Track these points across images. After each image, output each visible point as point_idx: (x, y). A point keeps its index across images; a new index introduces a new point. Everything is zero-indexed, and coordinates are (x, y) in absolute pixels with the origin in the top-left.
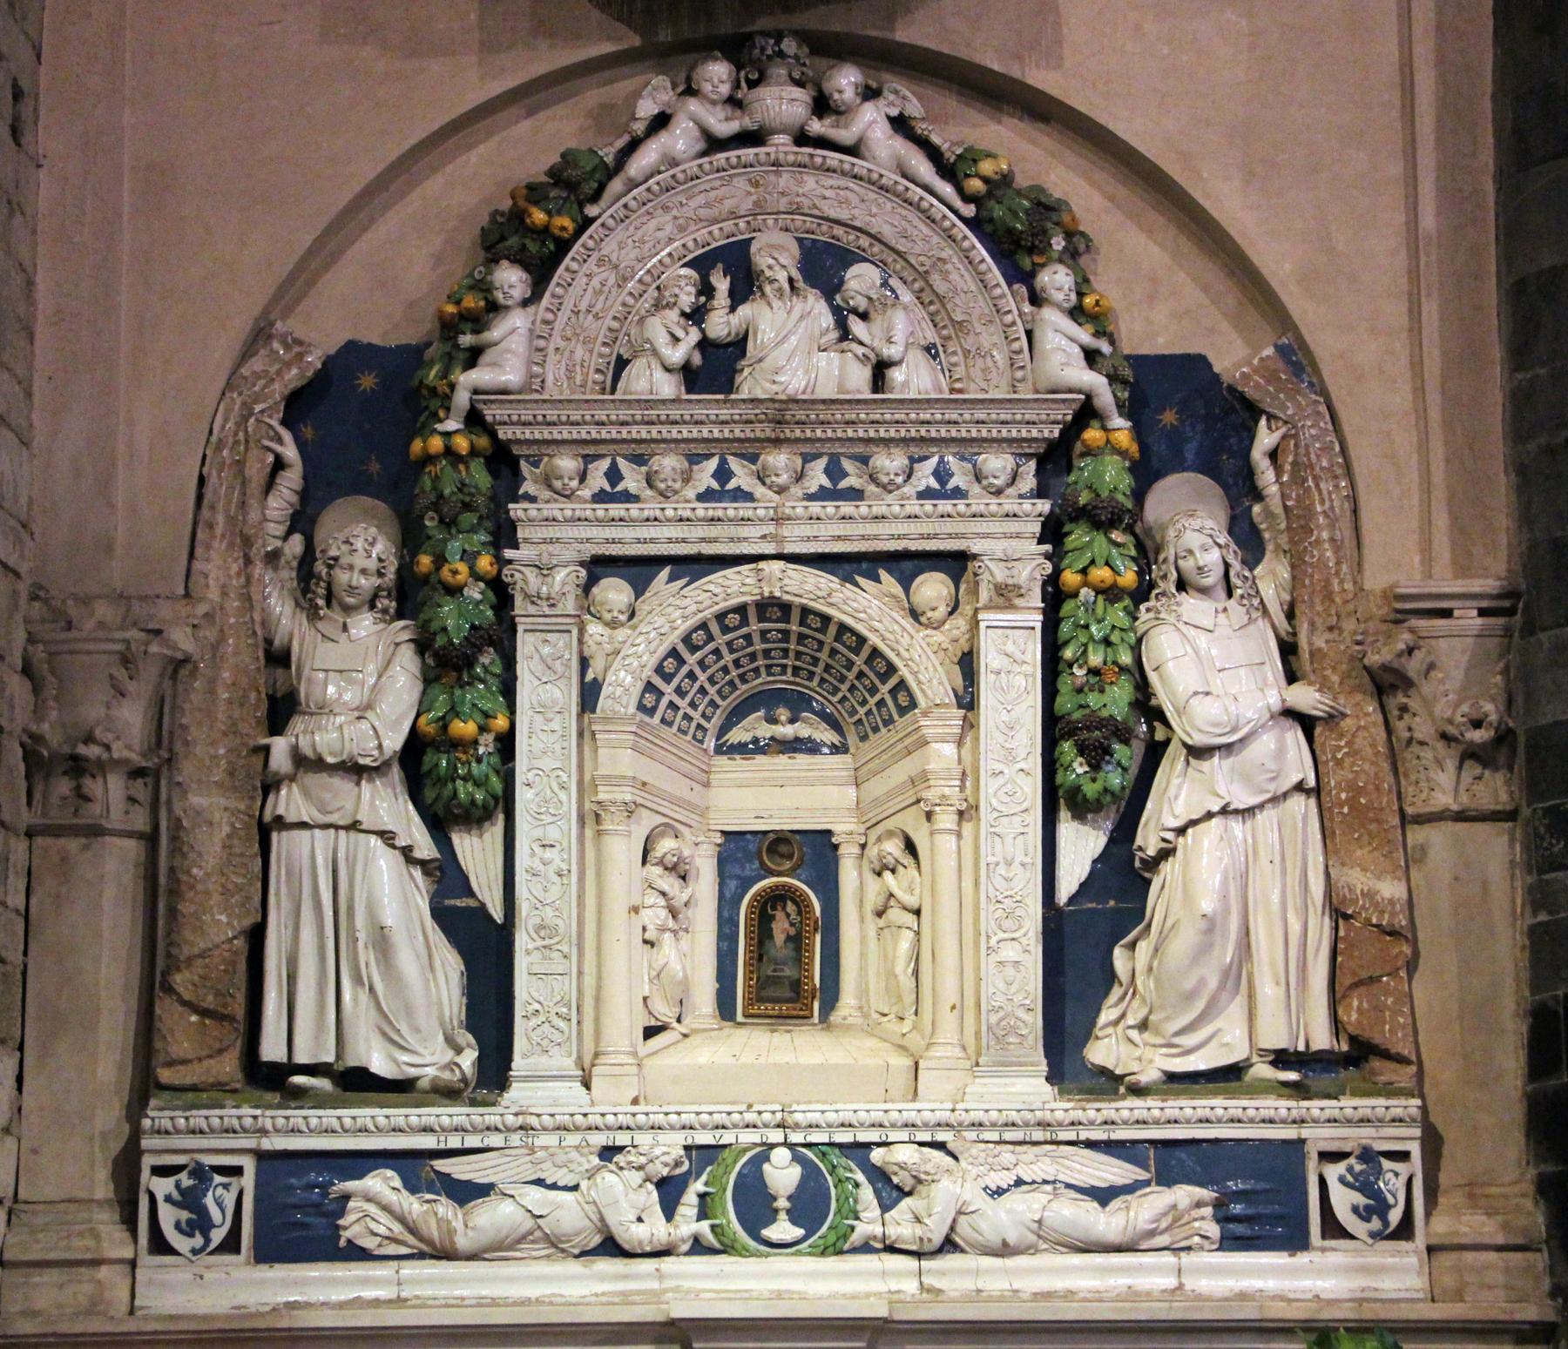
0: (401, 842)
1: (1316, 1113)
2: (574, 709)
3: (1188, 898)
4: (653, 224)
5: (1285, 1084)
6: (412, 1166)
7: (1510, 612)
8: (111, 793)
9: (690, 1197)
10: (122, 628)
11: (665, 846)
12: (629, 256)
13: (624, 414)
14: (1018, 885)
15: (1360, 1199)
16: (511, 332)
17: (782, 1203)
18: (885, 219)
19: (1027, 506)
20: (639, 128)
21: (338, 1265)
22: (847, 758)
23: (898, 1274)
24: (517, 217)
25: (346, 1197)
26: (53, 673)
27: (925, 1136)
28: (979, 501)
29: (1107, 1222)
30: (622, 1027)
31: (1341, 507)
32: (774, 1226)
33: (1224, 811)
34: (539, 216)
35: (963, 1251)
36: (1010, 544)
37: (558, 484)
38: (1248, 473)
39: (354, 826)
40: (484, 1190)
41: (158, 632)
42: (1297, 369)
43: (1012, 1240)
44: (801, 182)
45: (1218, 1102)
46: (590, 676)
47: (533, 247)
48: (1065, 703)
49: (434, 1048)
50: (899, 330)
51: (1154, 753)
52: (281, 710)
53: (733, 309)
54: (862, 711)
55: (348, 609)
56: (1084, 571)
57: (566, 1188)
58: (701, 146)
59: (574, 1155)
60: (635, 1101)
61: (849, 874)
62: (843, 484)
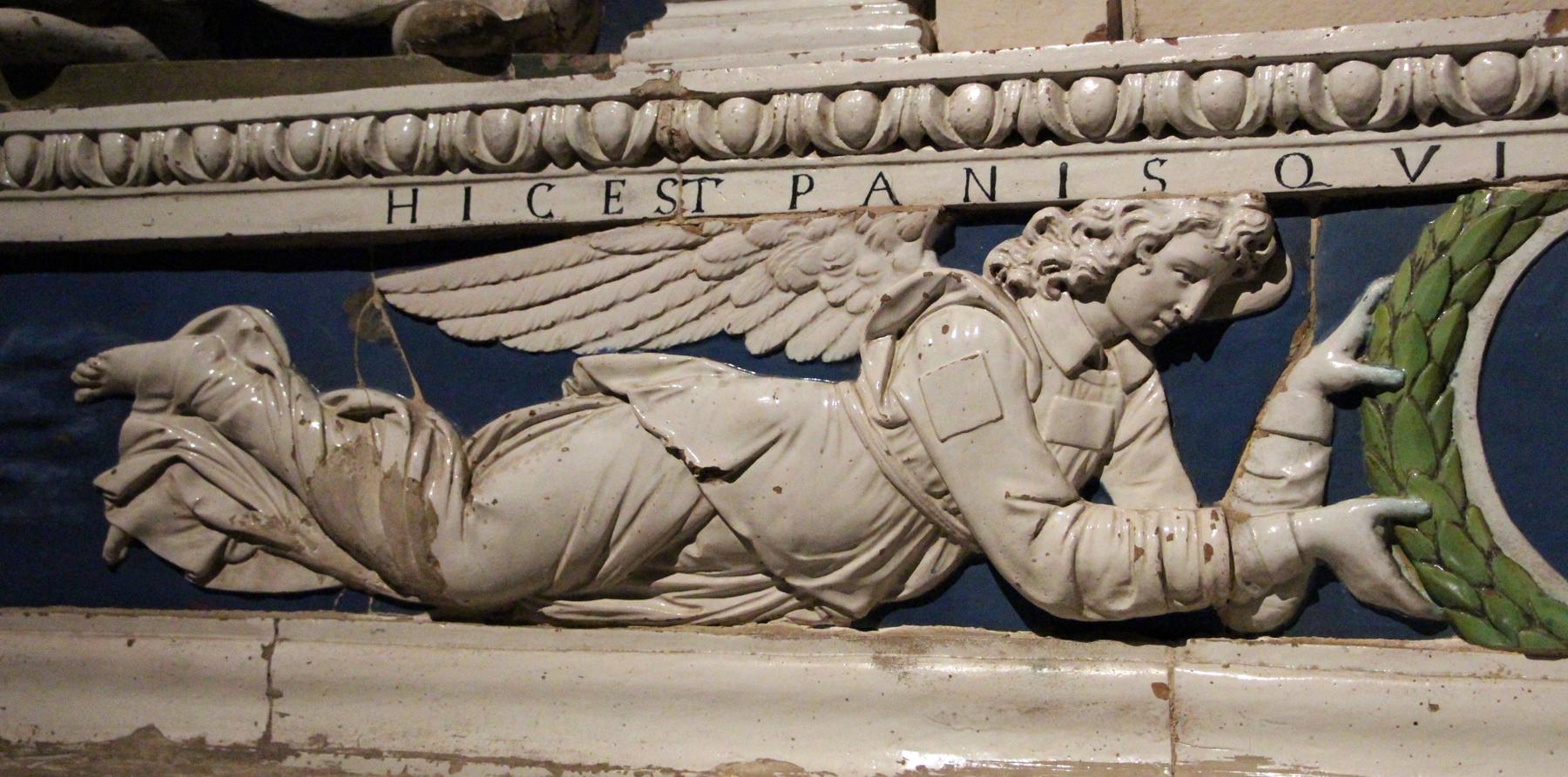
6: (322, 293)
9: (1294, 404)
21: (106, 618)
25: (121, 397)
57: (816, 368)
59: (842, 241)
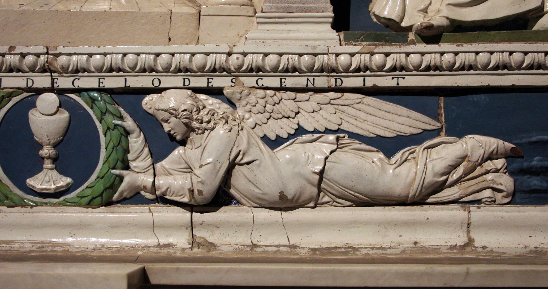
27: (201, 82)
32: (40, 175)
35: (238, 203)
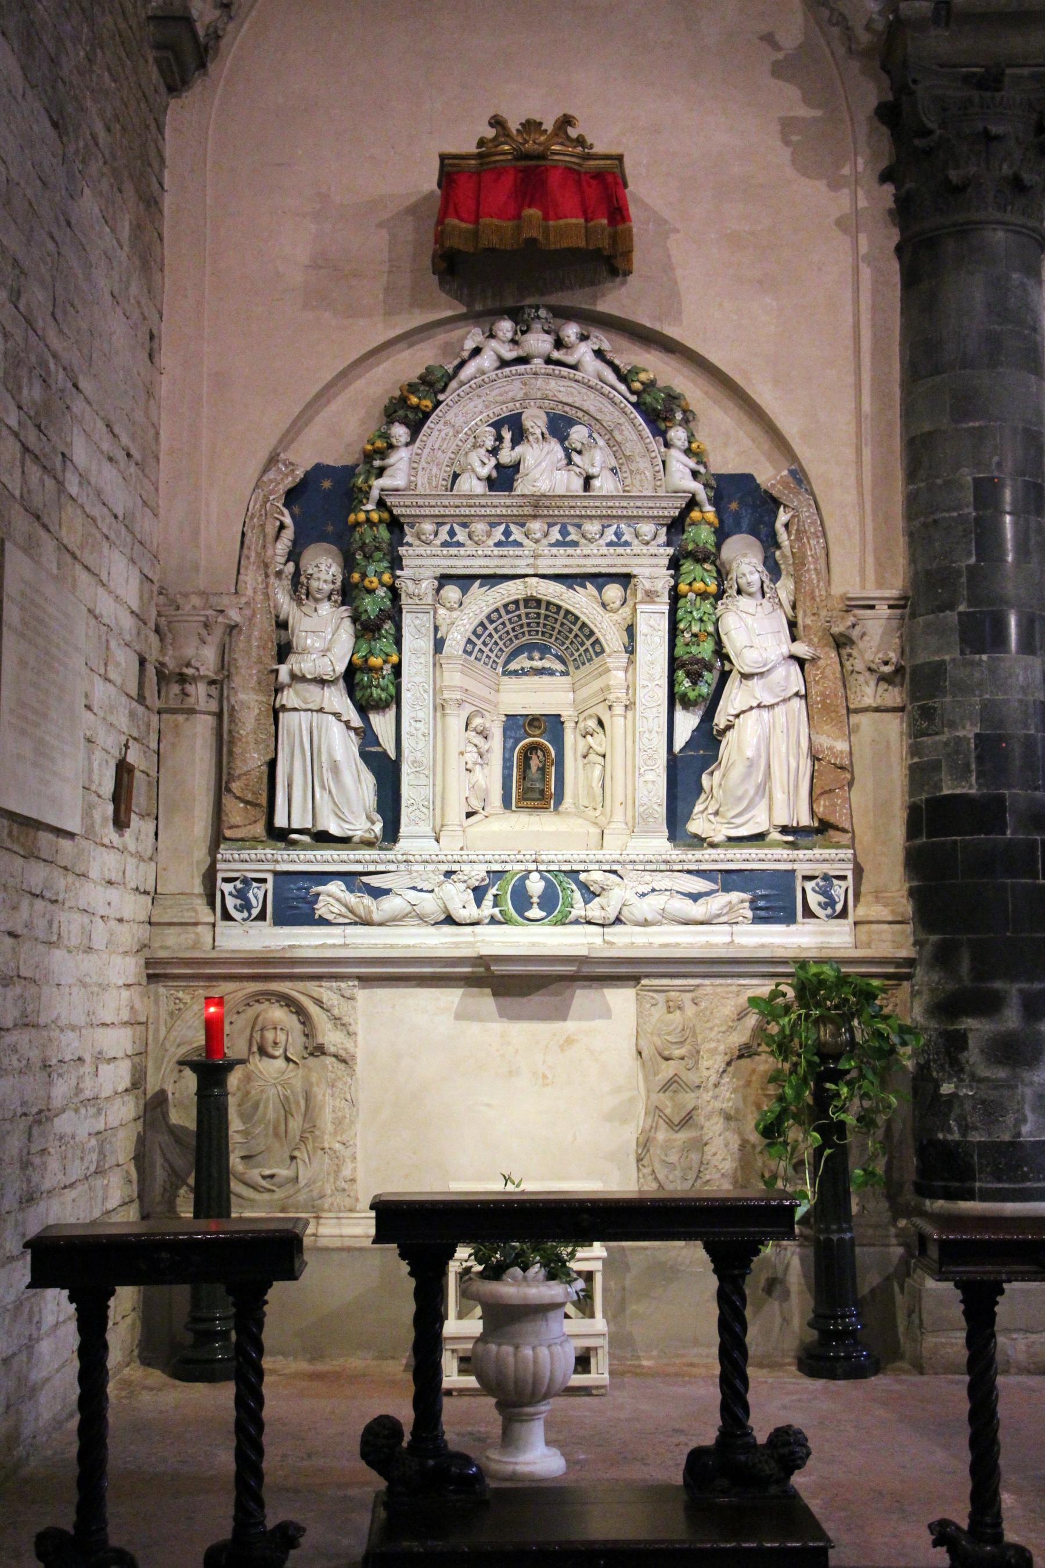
0: (344, 718)
1: (801, 856)
2: (432, 652)
3: (740, 749)
4: (472, 404)
5: (787, 842)
7: (904, 607)
8: (199, 693)
9: (489, 897)
10: (203, 609)
11: (477, 722)
12: (459, 421)
13: (457, 502)
14: (655, 742)
15: (822, 899)
16: (400, 459)
17: (535, 900)
18: (591, 402)
19: (662, 550)
20: (465, 354)
22: (568, 678)
23: (592, 935)
24: (403, 400)
26: (170, 631)
27: (607, 868)
28: (637, 547)
29: (697, 910)
30: (455, 812)
31: (820, 553)
33: (759, 706)
34: (414, 400)
36: (652, 569)
37: (423, 537)
38: (774, 535)
39: (321, 710)
40: (387, 892)
41: (222, 611)
42: (799, 482)
43: (649, 918)
44: (548, 384)
45: (753, 851)
46: (439, 636)
47: (411, 416)
48: (679, 651)
49: (362, 822)
50: (597, 460)
51: (724, 676)
52: (284, 651)
53: (513, 448)
54: (576, 654)
55: (317, 600)
56: (690, 584)
58: (497, 364)
59: (431, 875)
60: (462, 849)
61: (569, 737)
62: (568, 539)
